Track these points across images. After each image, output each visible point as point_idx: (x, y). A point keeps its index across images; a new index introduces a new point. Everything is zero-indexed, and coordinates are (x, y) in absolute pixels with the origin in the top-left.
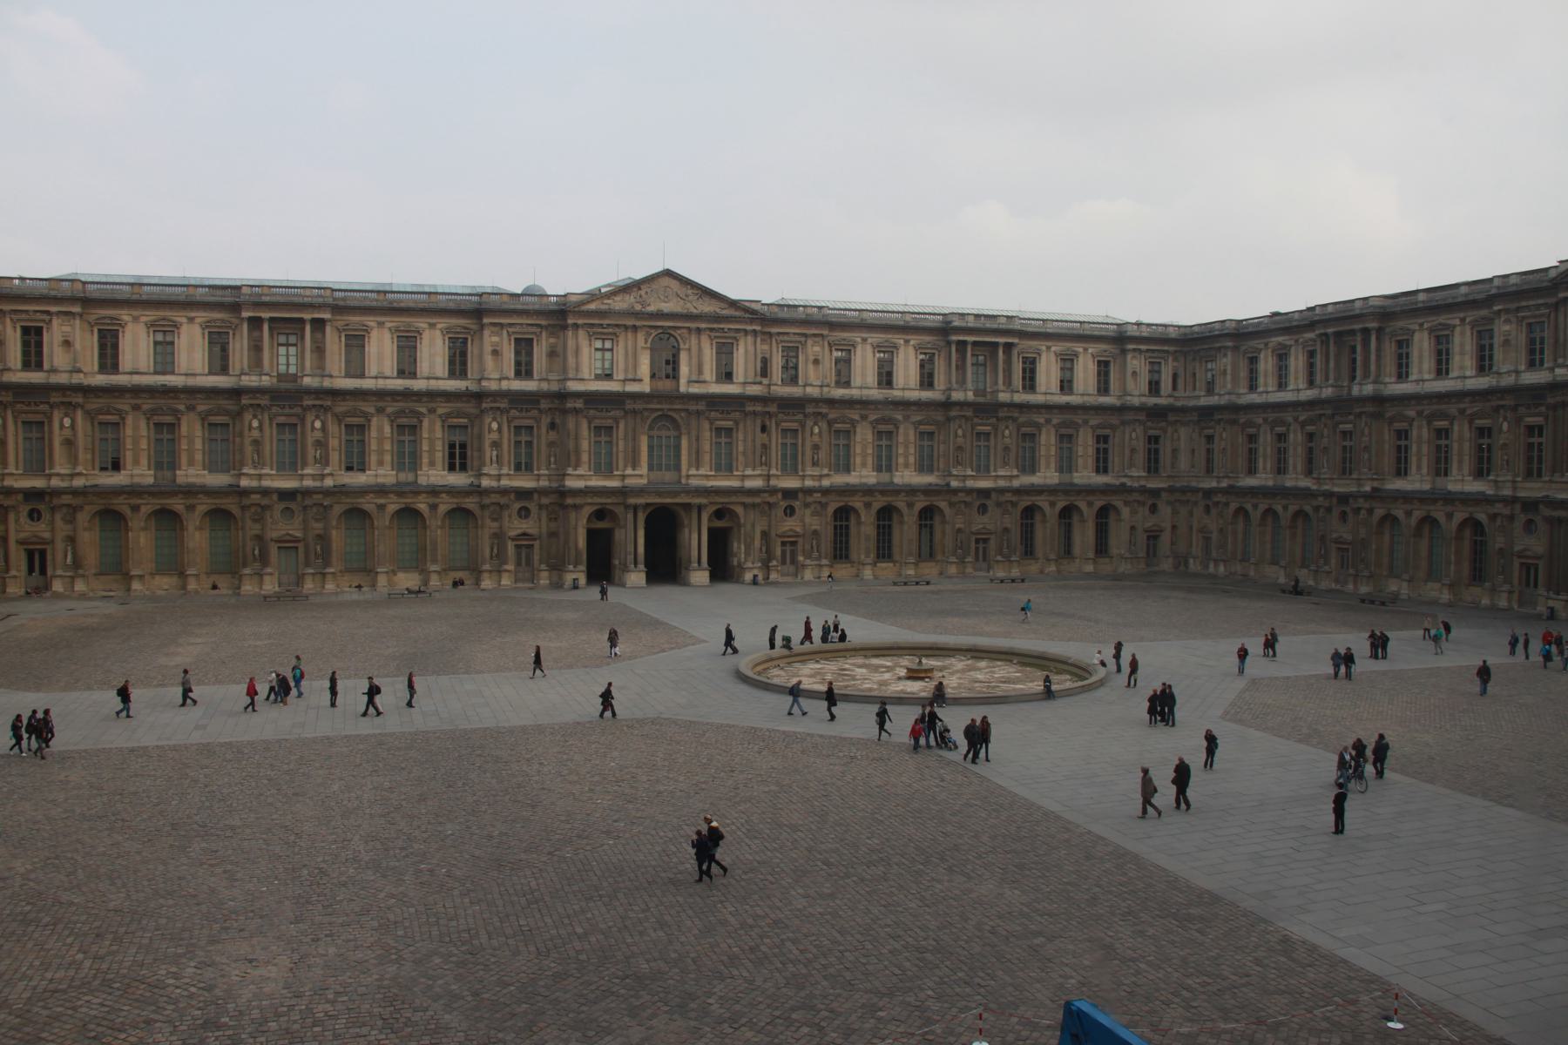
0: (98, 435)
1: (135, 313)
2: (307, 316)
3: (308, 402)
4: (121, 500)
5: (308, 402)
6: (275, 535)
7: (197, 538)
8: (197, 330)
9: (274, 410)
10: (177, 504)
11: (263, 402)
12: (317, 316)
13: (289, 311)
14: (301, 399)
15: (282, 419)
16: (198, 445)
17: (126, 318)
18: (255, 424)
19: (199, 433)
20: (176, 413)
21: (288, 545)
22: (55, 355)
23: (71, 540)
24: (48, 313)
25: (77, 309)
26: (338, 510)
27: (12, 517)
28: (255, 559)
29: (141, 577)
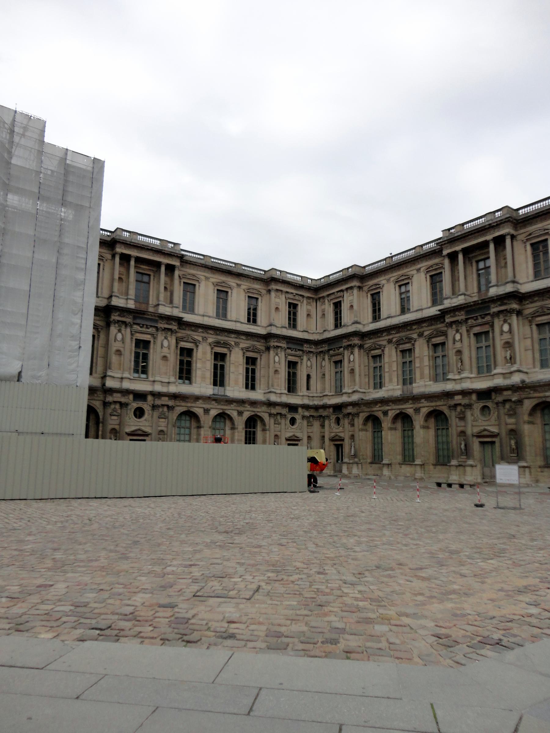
0: (372, 365)
1: (387, 277)
2: (489, 237)
3: (494, 309)
4: (377, 408)
5: (494, 309)
6: (476, 430)
7: (424, 436)
8: (422, 275)
9: (470, 322)
10: (409, 408)
11: (459, 318)
12: (497, 234)
13: (476, 238)
14: (488, 308)
15: (477, 330)
16: (426, 362)
17: (384, 282)
18: (458, 337)
19: (426, 353)
20: (410, 340)
21: (487, 440)
22: (347, 317)
23: (352, 437)
24: (342, 291)
25: (355, 283)
26: (528, 404)
27: (327, 422)
28: (462, 454)
29: (389, 465)
